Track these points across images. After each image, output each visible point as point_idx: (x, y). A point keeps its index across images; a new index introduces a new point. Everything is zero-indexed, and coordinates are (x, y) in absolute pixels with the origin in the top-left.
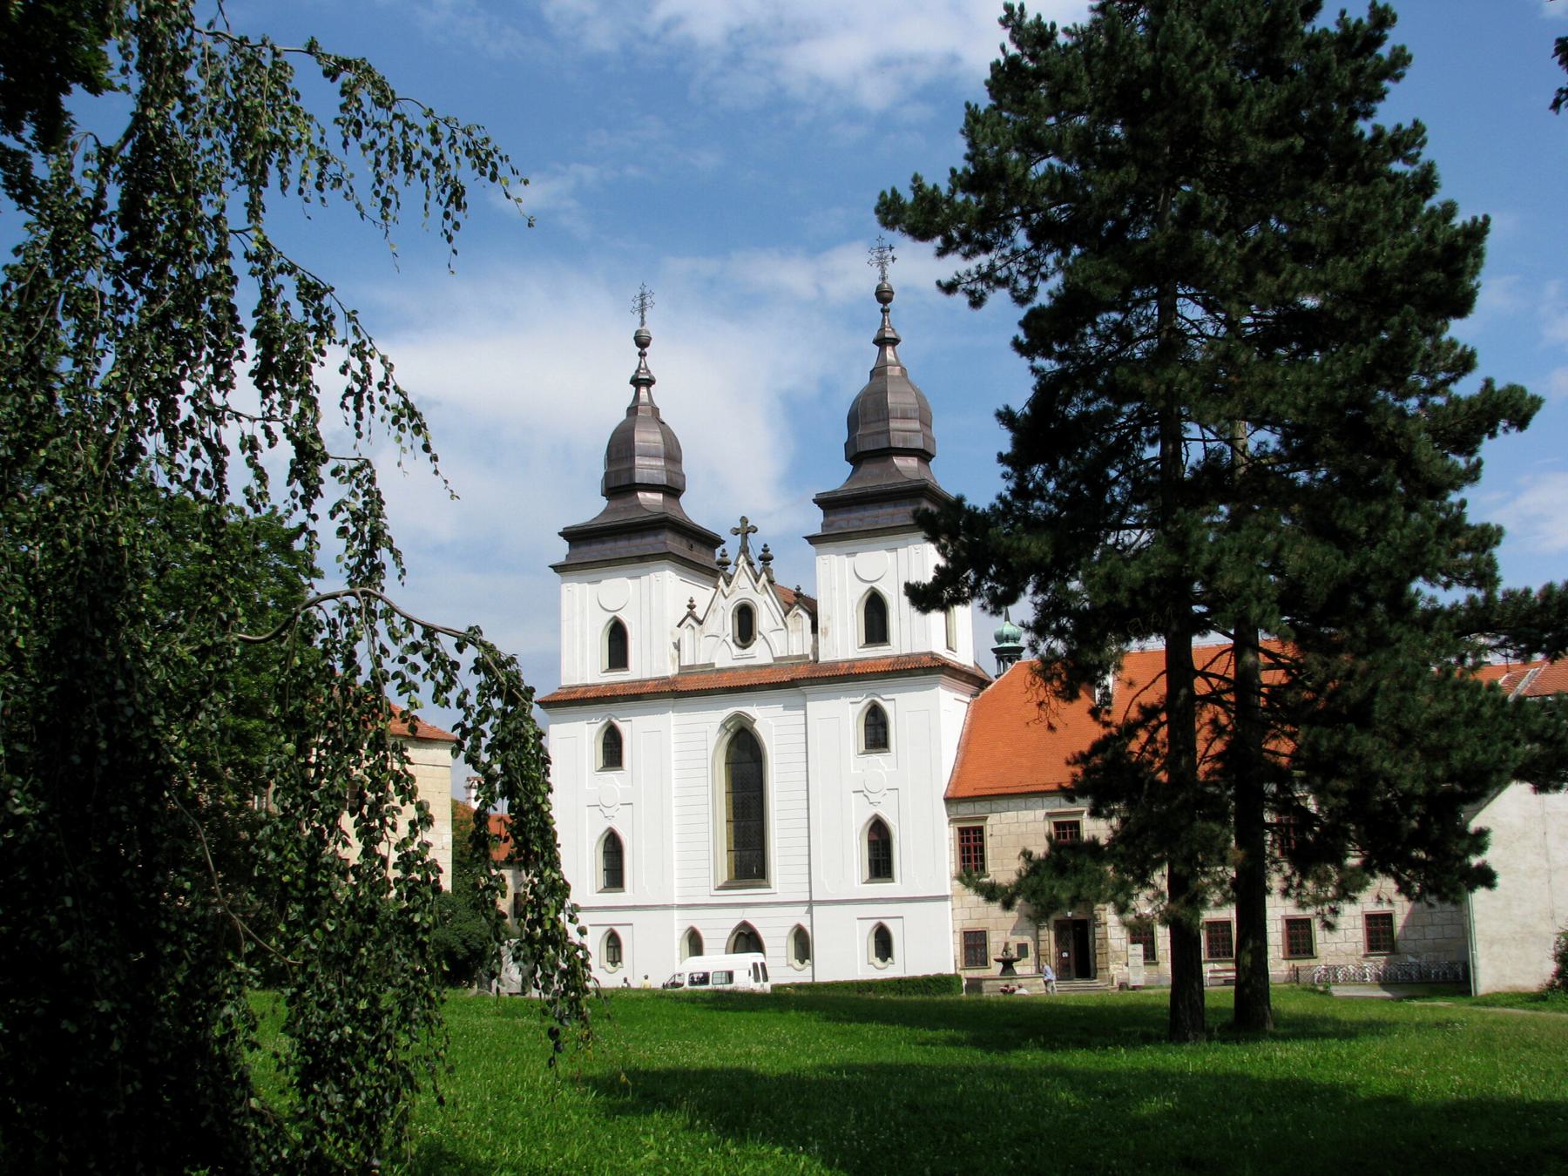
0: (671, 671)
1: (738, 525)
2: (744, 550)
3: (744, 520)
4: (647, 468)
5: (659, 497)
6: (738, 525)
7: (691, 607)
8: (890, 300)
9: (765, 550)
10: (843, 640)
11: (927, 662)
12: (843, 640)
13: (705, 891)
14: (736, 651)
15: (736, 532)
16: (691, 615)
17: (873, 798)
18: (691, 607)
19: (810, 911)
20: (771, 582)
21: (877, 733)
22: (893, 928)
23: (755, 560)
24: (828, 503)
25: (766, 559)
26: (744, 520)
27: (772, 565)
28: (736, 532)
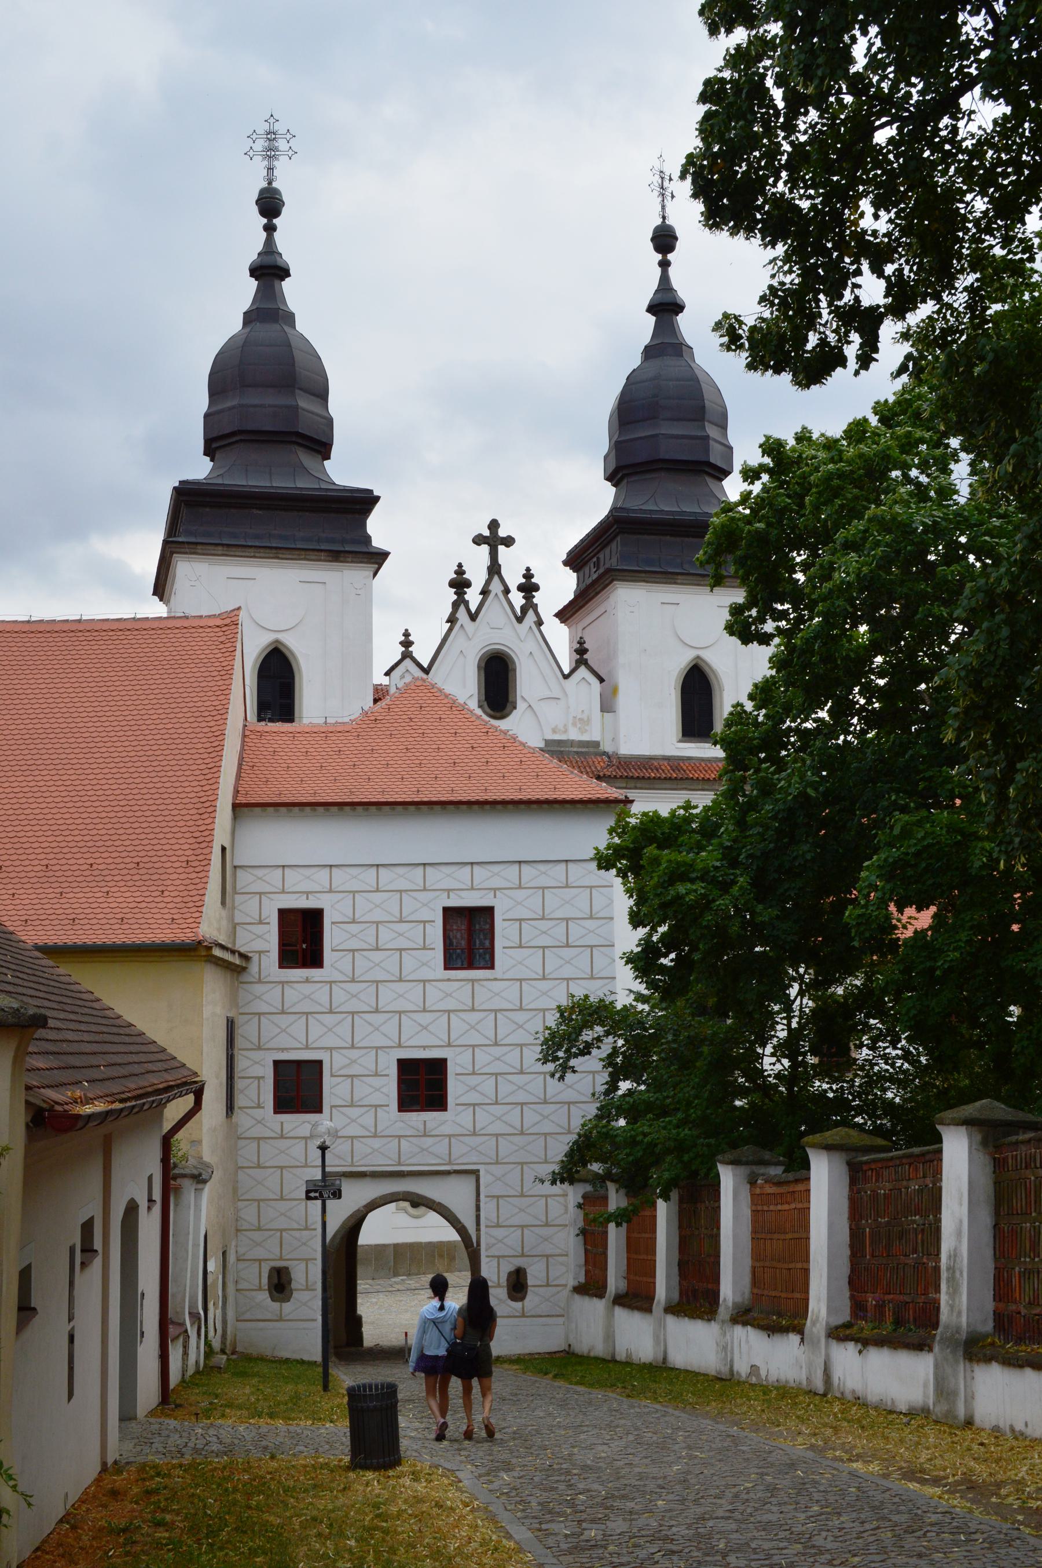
1: (502, 533)
2: (494, 569)
3: (494, 525)
6: (502, 533)
7: (407, 643)
8: (671, 249)
9: (528, 575)
15: (479, 540)
16: (407, 655)
18: (407, 643)
20: (540, 623)
23: (513, 587)
25: (529, 588)
26: (494, 525)
27: (538, 598)
28: (479, 540)
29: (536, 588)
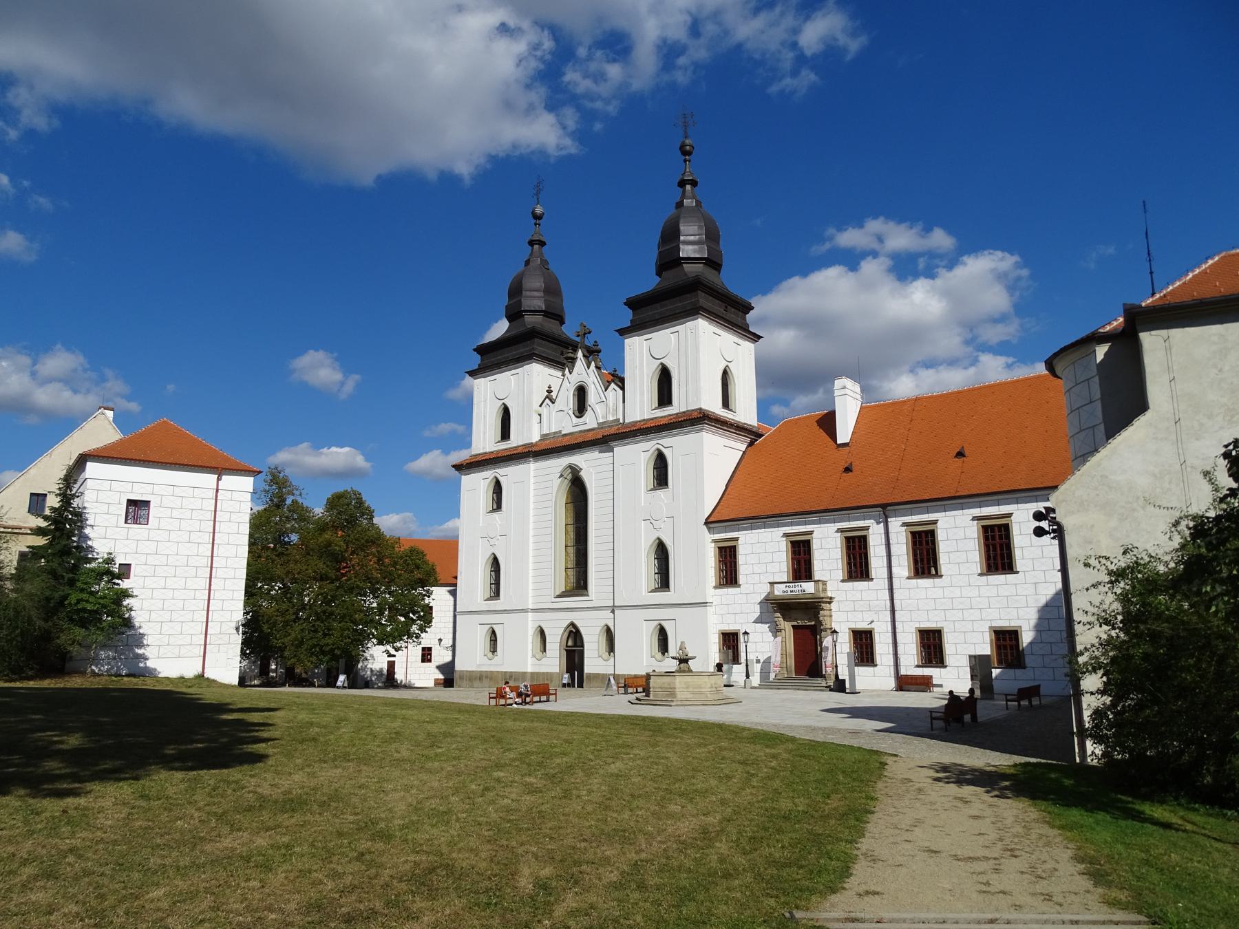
0: (535, 438)
4: (534, 300)
5: (539, 318)
7: (549, 391)
10: (639, 403)
11: (695, 415)
12: (639, 403)
13: (549, 601)
14: (575, 420)
17: (656, 524)
18: (549, 391)
19: (613, 612)
21: (661, 474)
22: (668, 627)
24: (634, 304)
29: (599, 351)
